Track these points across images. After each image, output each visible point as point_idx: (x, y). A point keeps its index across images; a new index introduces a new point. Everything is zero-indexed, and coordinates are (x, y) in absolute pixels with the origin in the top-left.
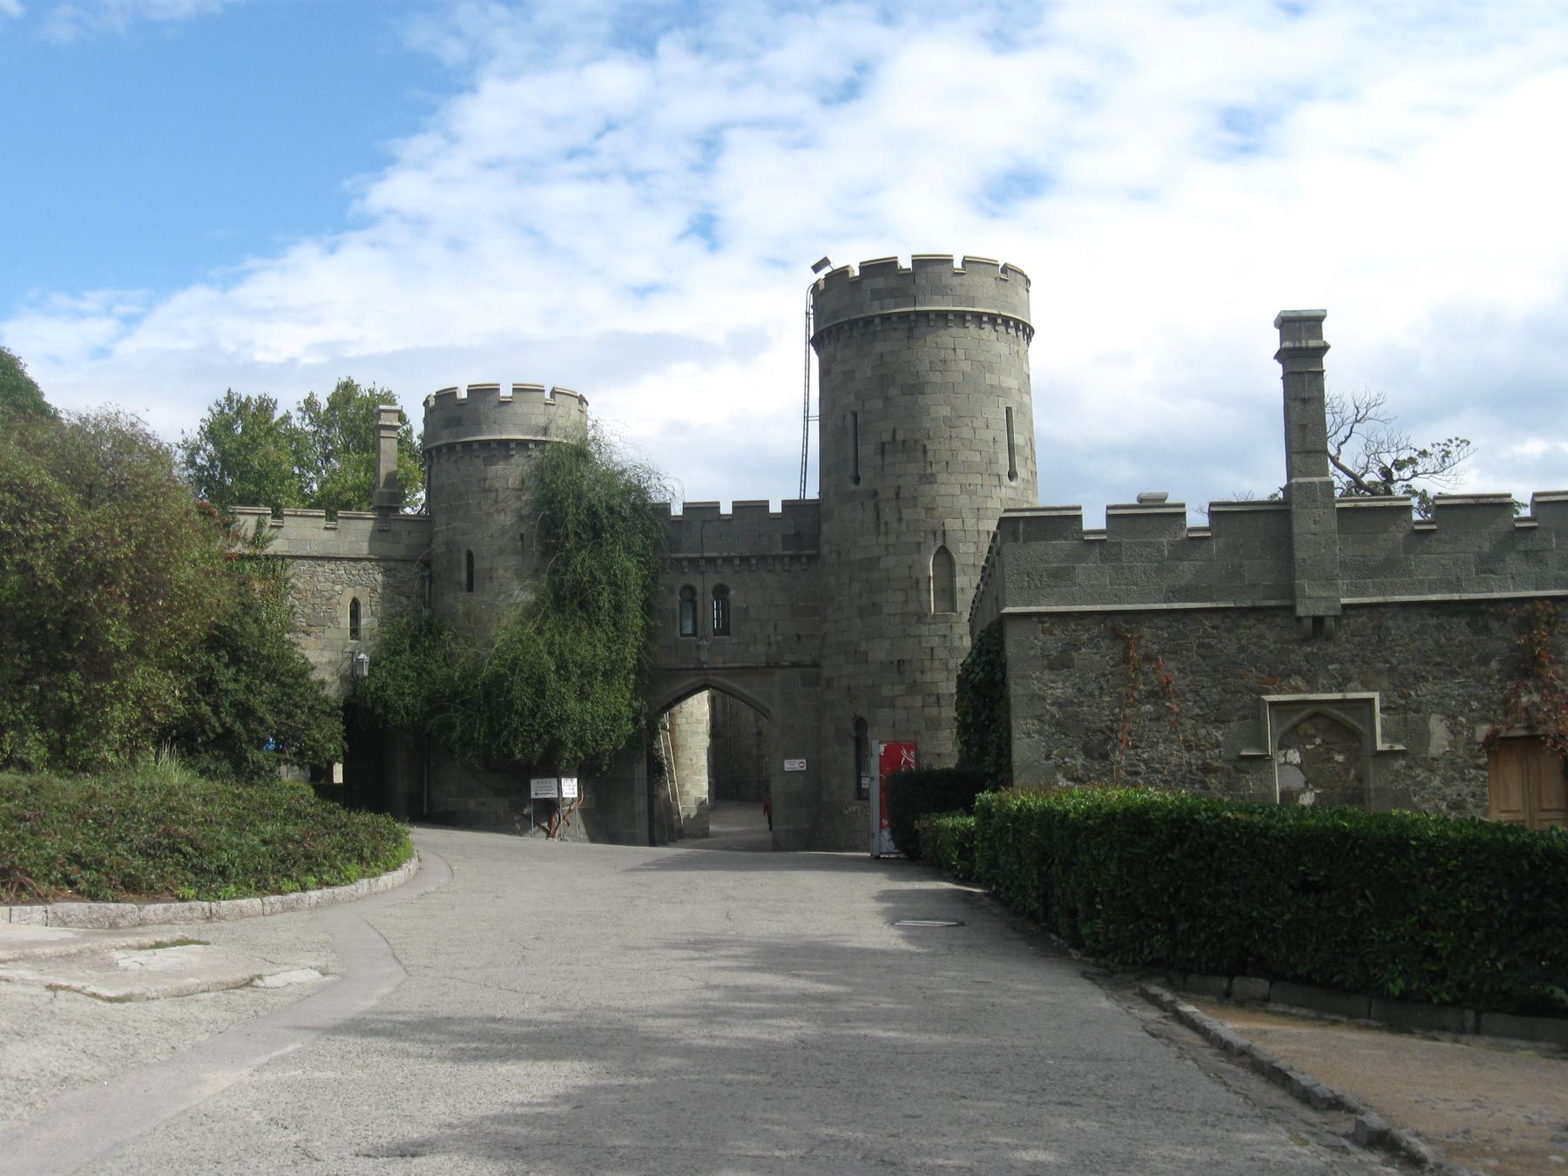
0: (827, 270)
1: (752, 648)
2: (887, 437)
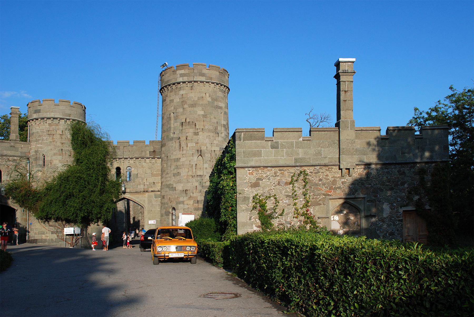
1: (139, 186)
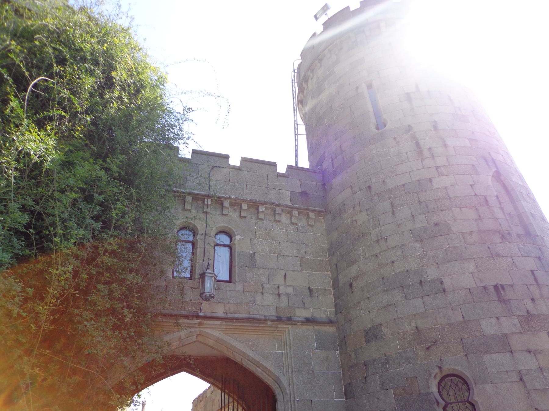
0: (324, 19)
1: (259, 297)
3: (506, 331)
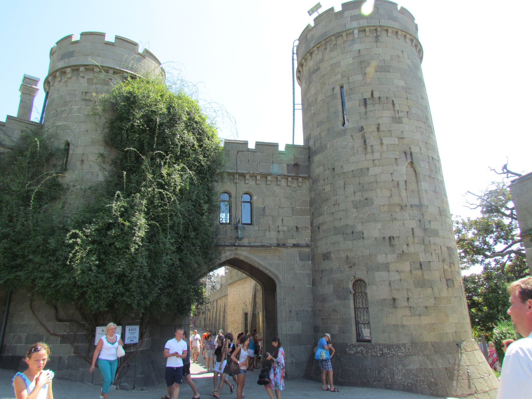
0: (315, 15)
2: (368, 95)
3: (389, 261)
